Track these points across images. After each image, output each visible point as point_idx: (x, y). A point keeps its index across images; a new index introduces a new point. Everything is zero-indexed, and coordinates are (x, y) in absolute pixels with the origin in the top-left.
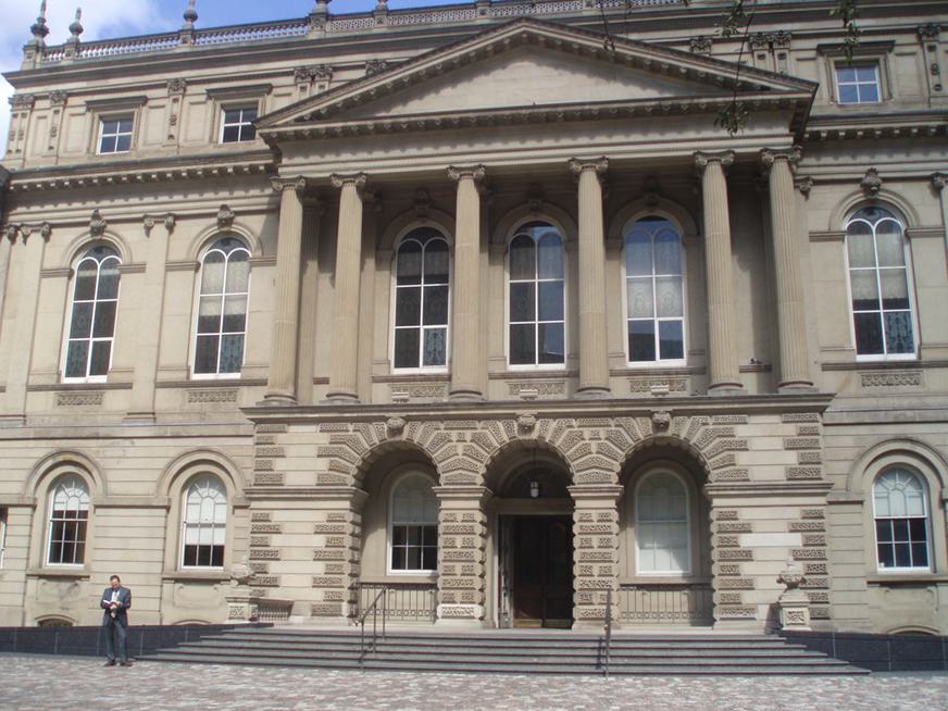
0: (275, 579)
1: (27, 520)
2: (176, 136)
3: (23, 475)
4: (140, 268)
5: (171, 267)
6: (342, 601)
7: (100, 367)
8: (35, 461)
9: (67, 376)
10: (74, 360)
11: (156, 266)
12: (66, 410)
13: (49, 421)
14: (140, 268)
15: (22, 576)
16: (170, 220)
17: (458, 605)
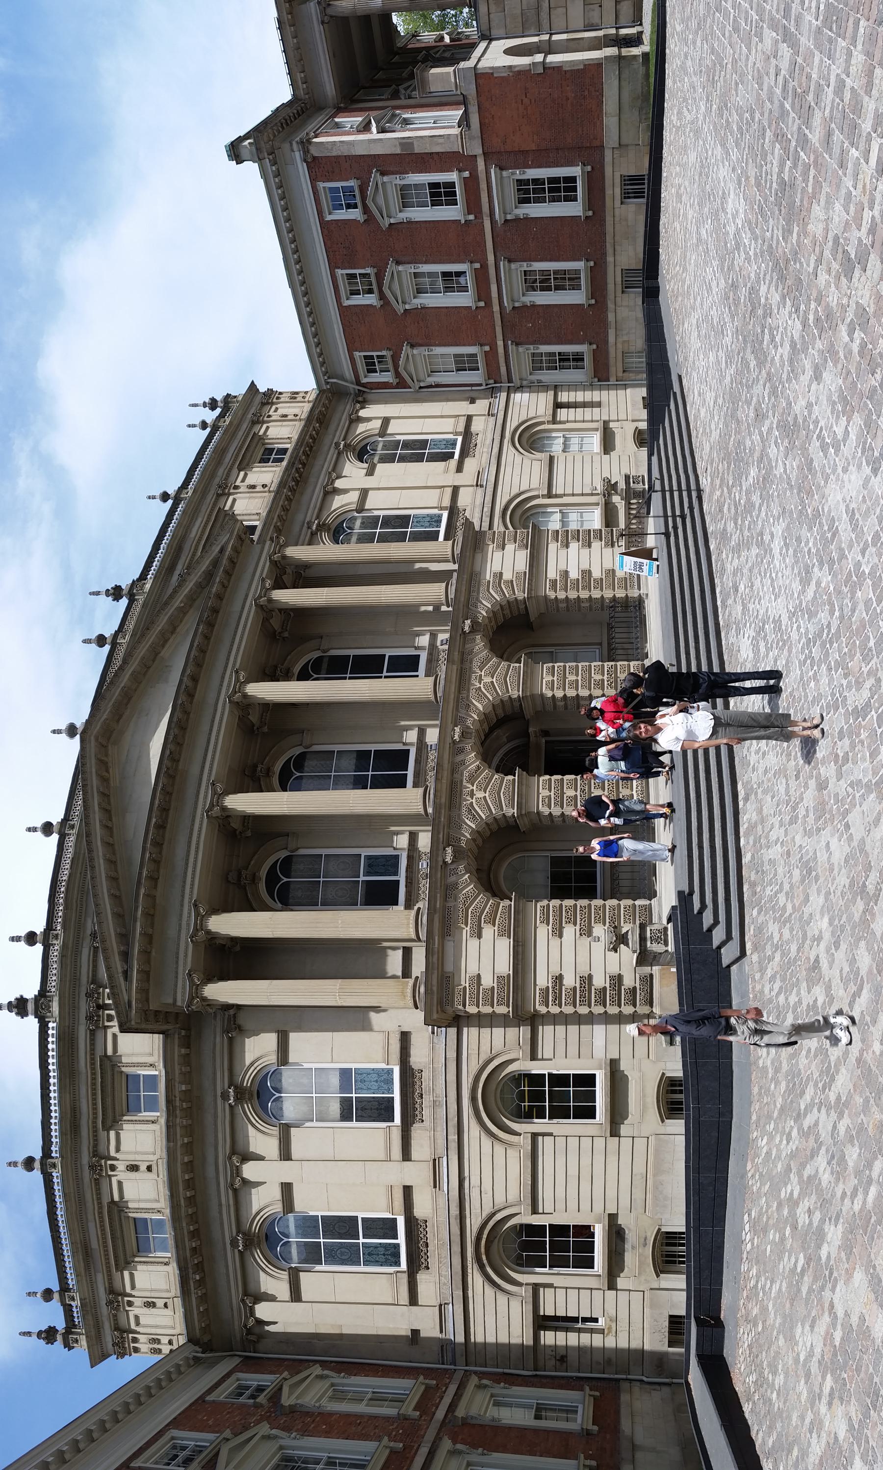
0: (612, 978)
1: (549, 1292)
2: (148, 1164)
3: (502, 1299)
4: (287, 1189)
5: (285, 1154)
6: (634, 905)
7: (387, 1227)
8: (487, 1286)
9: (399, 1265)
10: (382, 1258)
11: (285, 1172)
12: (433, 1261)
13: (445, 1277)
14: (287, 1189)
15: (611, 1294)
16: (235, 1159)
17: (634, 792)
